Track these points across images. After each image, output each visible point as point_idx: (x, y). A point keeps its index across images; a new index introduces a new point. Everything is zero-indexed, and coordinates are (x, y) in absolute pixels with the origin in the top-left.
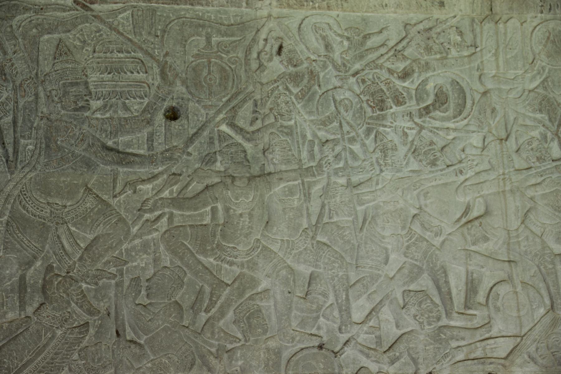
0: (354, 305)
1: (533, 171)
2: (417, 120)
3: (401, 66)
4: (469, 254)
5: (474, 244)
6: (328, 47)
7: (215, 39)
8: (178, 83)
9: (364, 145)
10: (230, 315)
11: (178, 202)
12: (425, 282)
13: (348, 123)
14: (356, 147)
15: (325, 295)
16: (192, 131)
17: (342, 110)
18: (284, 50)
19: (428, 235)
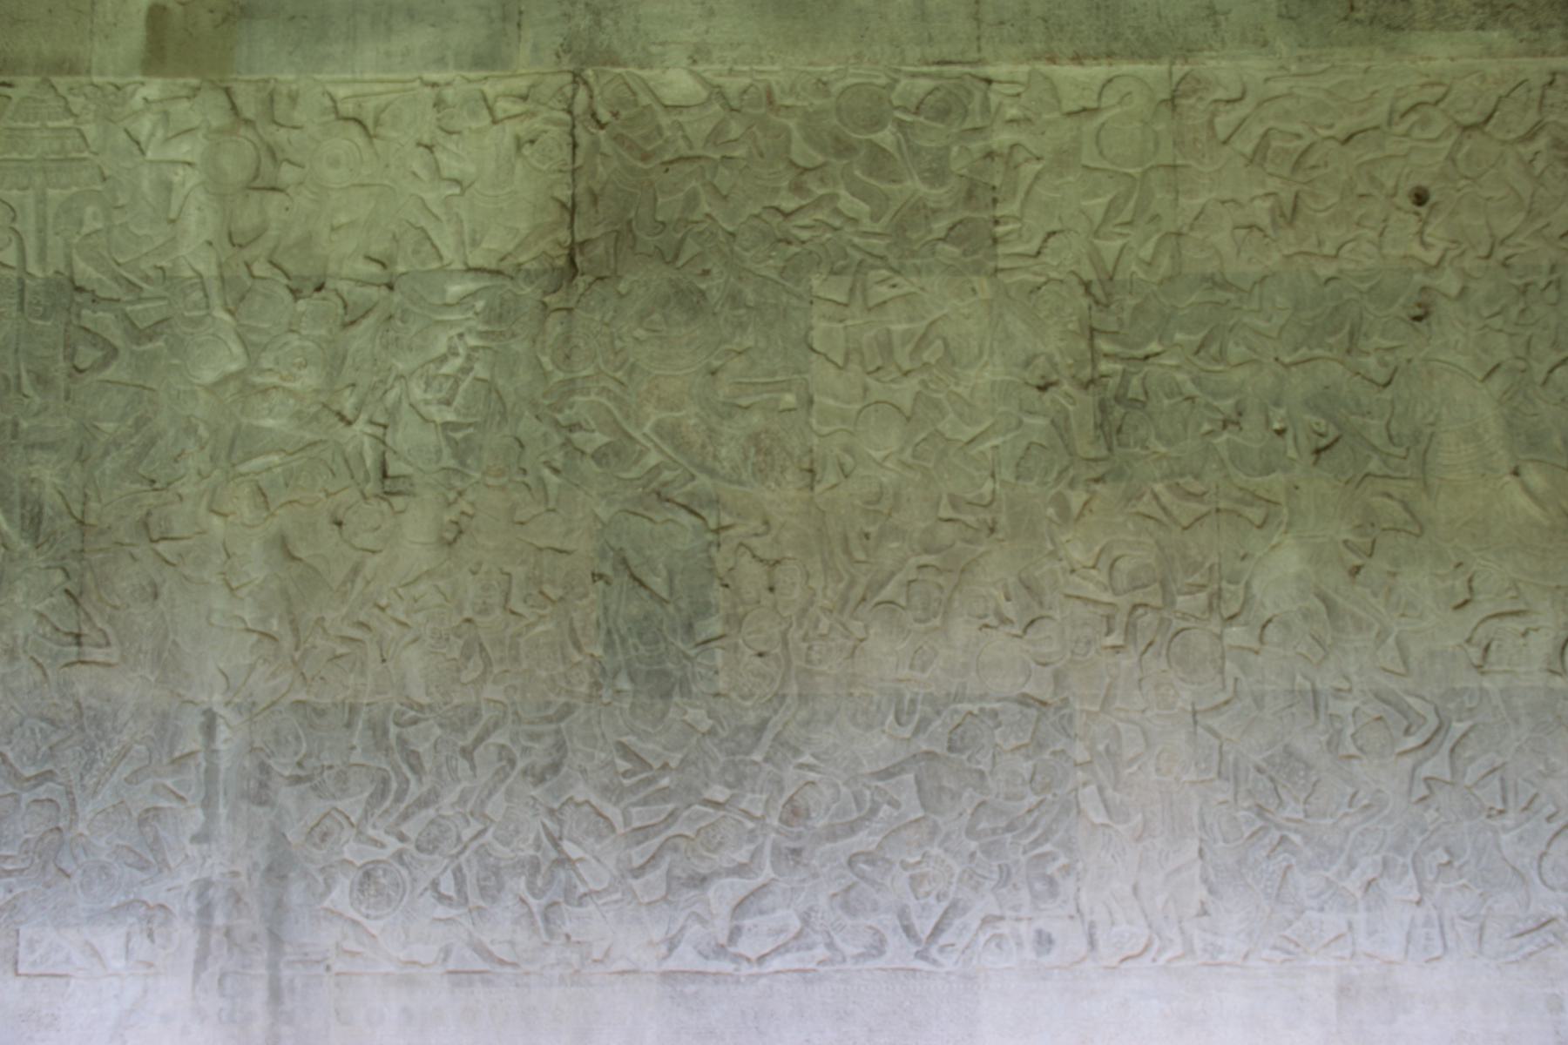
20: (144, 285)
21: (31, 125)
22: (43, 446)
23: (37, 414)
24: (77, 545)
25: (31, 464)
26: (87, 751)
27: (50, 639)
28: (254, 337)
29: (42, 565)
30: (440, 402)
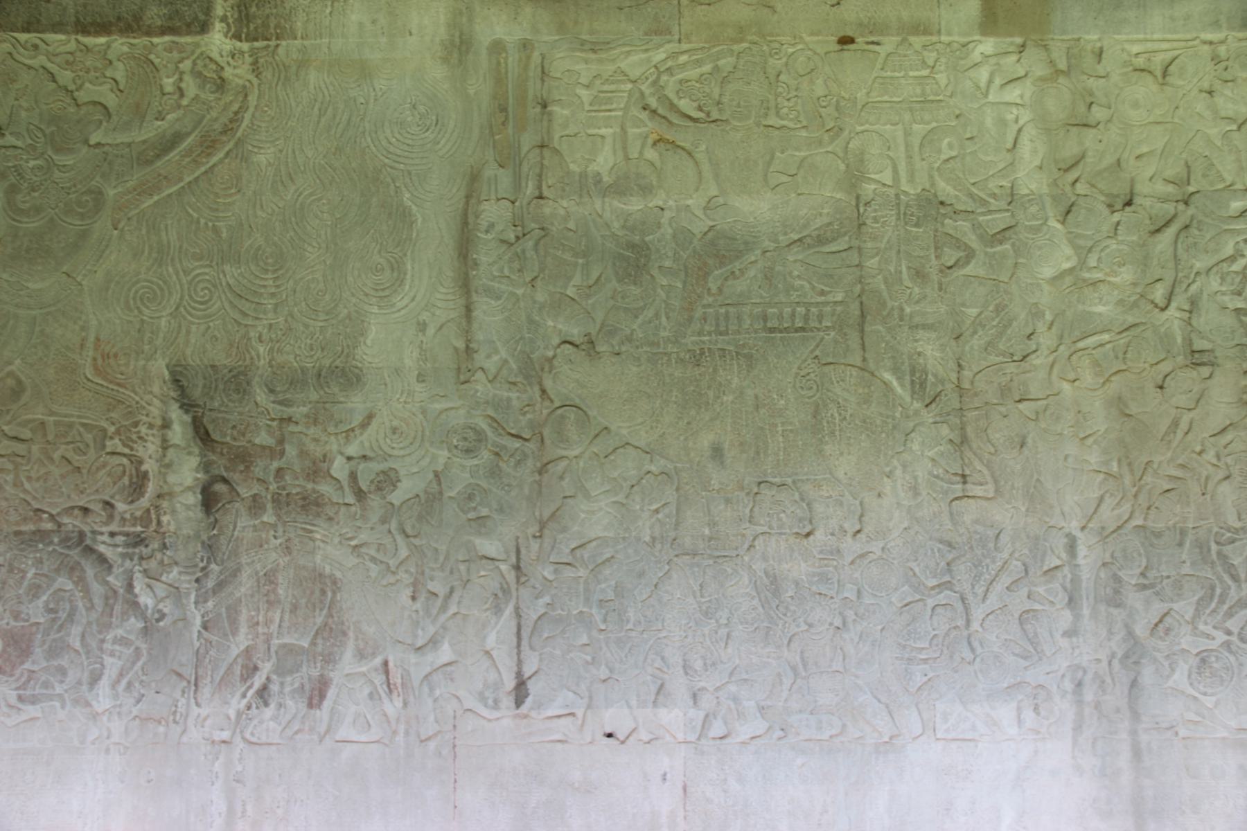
20: (992, 201)
21: (897, 74)
22: (925, 327)
23: (917, 302)
24: (958, 406)
25: (916, 341)
26: (976, 566)
27: (942, 479)
28: (1081, 242)
29: (931, 420)
30: (1233, 293)
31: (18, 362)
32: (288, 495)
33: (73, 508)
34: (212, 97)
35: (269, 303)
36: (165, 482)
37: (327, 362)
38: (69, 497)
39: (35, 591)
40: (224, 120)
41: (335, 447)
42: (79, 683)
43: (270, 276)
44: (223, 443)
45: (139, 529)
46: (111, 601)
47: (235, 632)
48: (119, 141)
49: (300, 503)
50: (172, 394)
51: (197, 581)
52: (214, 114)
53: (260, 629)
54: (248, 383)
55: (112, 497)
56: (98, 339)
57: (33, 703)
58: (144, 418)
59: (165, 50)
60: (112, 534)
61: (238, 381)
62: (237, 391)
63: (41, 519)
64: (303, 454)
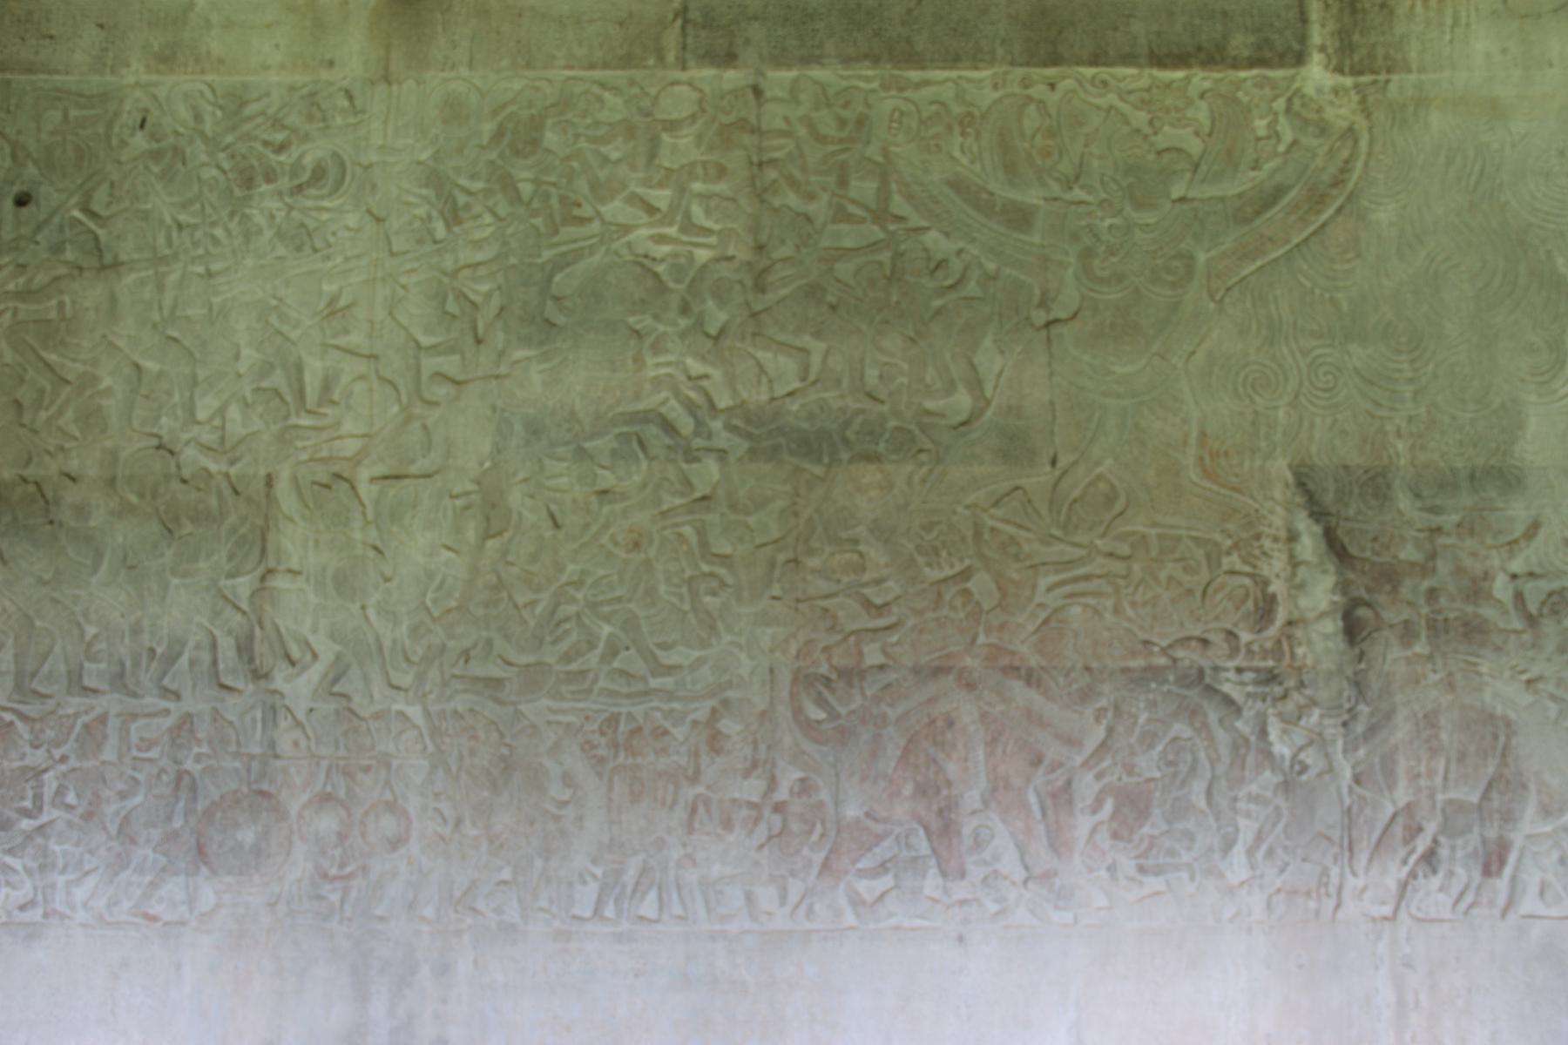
0: (199, 404)
1: (410, 256)
2: (287, 199)
3: (279, 137)
4: (326, 347)
5: (334, 336)
6: (198, 117)
7: (74, 113)
8: (30, 164)
9: (228, 231)
10: (69, 414)
11: (23, 295)
12: (278, 379)
13: (212, 206)
14: (219, 232)
15: (169, 394)
16: (42, 218)
17: (205, 190)
18: (148, 125)
19: (285, 328)
31: (1109, 462)
32: (1446, 620)
33: (1189, 639)
34: (1315, 142)
35: (1407, 391)
36: (1297, 606)
37: (1480, 461)
38: (1182, 624)
39: (1149, 739)
40: (1332, 169)
41: (1496, 562)
42: (1210, 849)
43: (1404, 357)
44: (1363, 560)
45: (1270, 663)
46: (1242, 751)
47: (1391, 786)
48: (1208, 195)
49: (1461, 630)
50: (1299, 500)
51: (1345, 724)
52: (1319, 162)
53: (1423, 782)
54: (1389, 486)
55: (1236, 625)
56: (1203, 435)
57: (1157, 874)
58: (1267, 530)
59: (1256, 85)
60: (1239, 670)
61: (1376, 484)
62: (1376, 496)
63: (1151, 653)
64: (1459, 571)
